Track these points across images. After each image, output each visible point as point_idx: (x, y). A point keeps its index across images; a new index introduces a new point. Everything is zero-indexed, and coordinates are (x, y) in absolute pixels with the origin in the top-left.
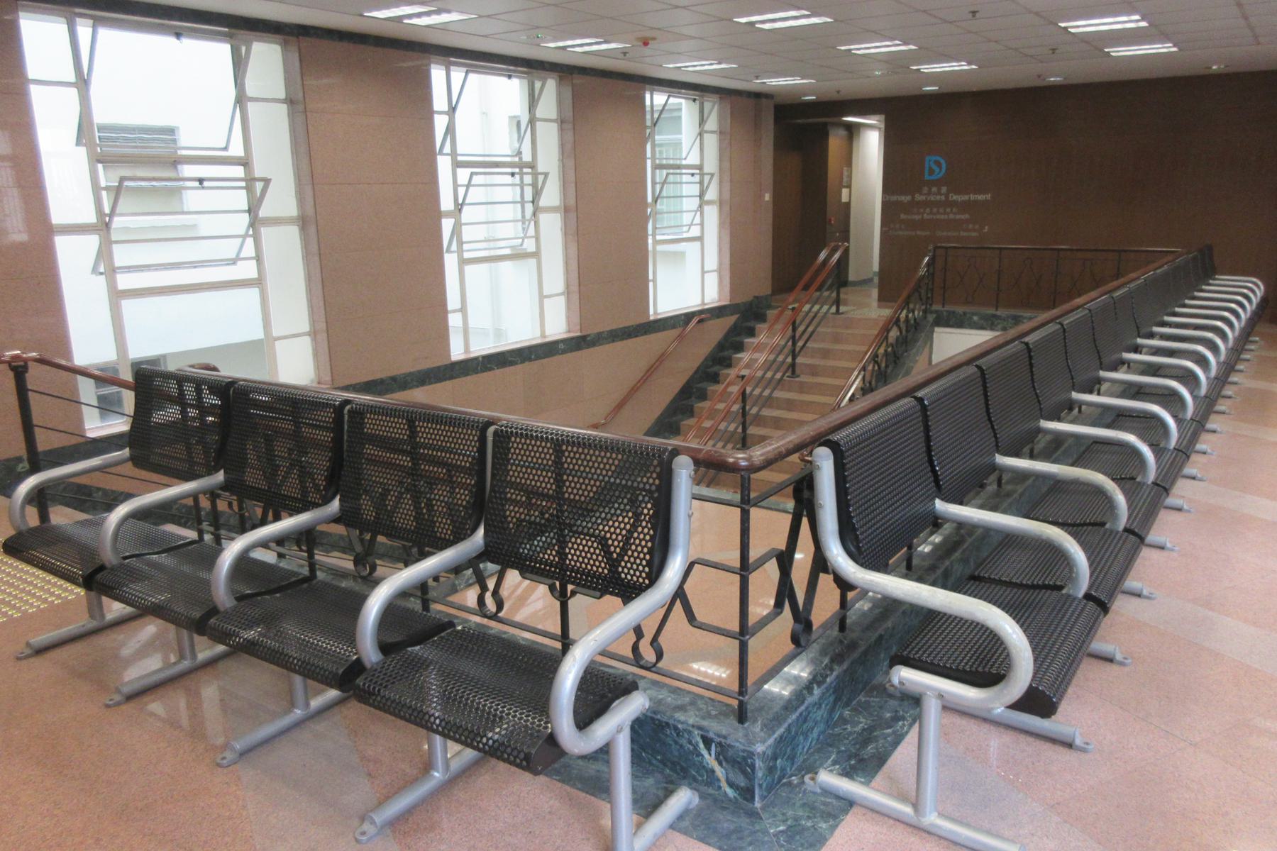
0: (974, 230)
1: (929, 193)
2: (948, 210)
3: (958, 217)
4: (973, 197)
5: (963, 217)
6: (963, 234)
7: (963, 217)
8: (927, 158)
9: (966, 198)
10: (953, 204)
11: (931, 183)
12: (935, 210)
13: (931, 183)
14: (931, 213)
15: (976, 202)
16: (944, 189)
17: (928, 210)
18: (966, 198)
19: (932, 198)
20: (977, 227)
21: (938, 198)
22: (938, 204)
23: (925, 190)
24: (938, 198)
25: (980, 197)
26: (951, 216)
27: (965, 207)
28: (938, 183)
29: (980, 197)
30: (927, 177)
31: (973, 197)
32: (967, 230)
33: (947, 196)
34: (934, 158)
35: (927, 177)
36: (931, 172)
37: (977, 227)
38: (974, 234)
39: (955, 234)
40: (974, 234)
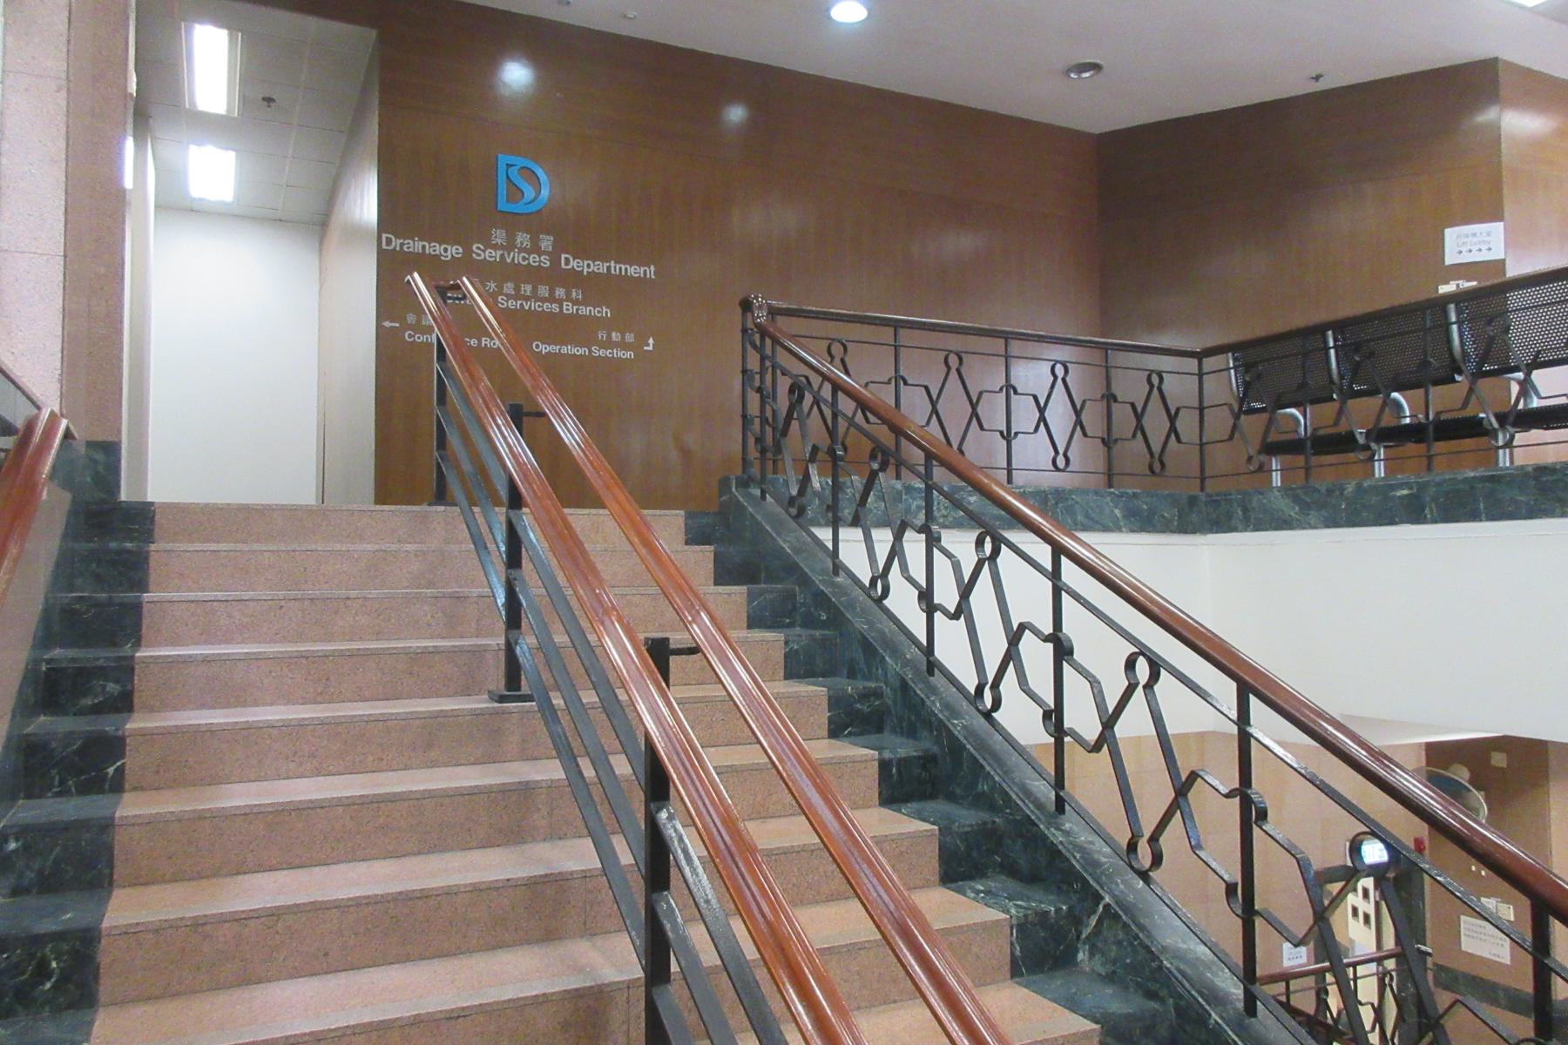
0: (623, 345)
1: (510, 246)
2: (560, 292)
3: (585, 311)
4: (616, 268)
5: (595, 312)
6: (598, 352)
7: (595, 312)
8: (503, 159)
9: (600, 267)
10: (574, 280)
11: (513, 222)
12: (527, 289)
13: (513, 222)
14: (517, 296)
15: (623, 279)
16: (546, 242)
17: (509, 288)
18: (600, 267)
19: (517, 257)
20: (630, 338)
21: (533, 259)
22: (535, 275)
23: (499, 236)
24: (533, 259)
25: (633, 271)
26: (568, 308)
27: (594, 288)
28: (535, 223)
29: (633, 271)
30: (503, 205)
31: (616, 268)
32: (609, 344)
33: (555, 261)
34: (521, 162)
35: (503, 205)
36: (515, 193)
37: (630, 338)
38: (629, 354)
39: (581, 351)
40: (629, 354)
